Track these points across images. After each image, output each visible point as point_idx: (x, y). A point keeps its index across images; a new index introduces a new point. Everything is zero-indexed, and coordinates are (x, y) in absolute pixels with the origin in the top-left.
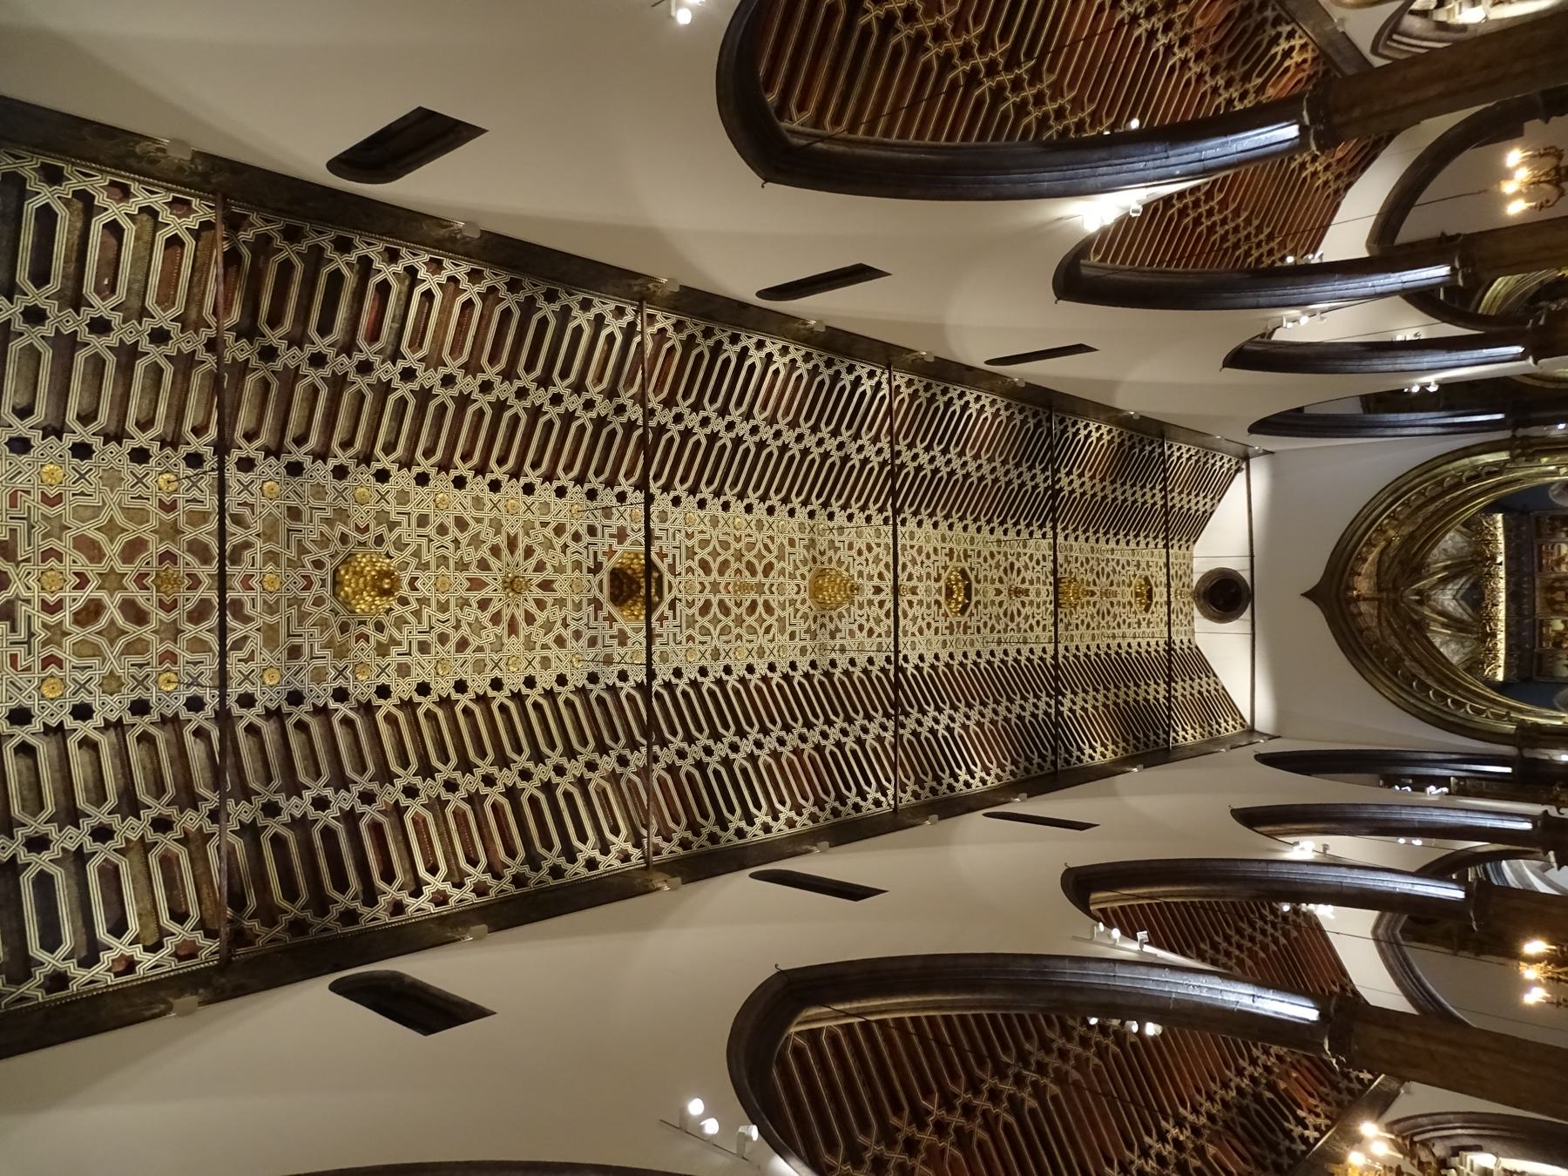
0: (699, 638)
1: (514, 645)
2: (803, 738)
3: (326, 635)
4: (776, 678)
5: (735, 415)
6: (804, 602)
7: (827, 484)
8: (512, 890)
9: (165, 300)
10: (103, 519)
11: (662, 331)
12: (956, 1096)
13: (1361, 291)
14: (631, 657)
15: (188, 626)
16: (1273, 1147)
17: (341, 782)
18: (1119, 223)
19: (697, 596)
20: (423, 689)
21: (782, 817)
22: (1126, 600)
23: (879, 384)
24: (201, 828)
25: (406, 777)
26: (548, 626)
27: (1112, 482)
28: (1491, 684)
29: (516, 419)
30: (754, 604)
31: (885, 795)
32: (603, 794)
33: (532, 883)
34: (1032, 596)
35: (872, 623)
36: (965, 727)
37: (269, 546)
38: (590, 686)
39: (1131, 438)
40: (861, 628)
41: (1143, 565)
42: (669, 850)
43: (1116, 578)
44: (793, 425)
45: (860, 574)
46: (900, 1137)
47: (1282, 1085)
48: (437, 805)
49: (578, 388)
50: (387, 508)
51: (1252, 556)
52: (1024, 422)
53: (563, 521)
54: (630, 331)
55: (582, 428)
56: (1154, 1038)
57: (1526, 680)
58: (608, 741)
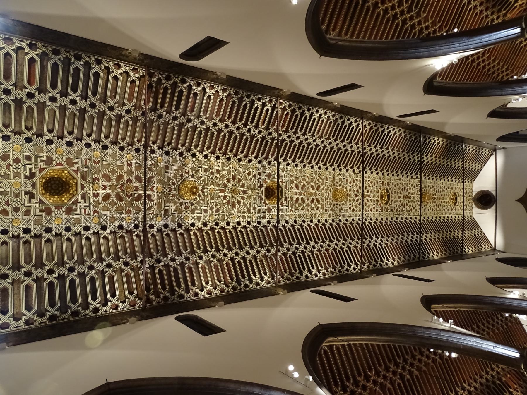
0: (294, 210)
1: (234, 211)
2: (329, 246)
3: (176, 206)
4: (320, 225)
5: (308, 135)
6: (330, 199)
7: (340, 159)
9: (130, 100)
10: (111, 168)
11: (284, 107)
12: (381, 372)
14: (272, 216)
15: (135, 202)
17: (180, 254)
18: (448, 66)
20: (205, 225)
22: (447, 201)
23: (358, 124)
24: (137, 266)
25: (199, 253)
27: (443, 159)
29: (236, 137)
30: (313, 200)
31: (357, 266)
32: (261, 261)
34: (412, 199)
35: (354, 207)
36: (386, 244)
37: (159, 178)
38: (258, 225)
39: (450, 143)
40: (350, 208)
41: (454, 188)
42: (283, 281)
43: (443, 193)
44: (328, 139)
45: (350, 190)
46: (360, 384)
47: (504, 379)
48: (209, 262)
49: (256, 127)
50: (195, 166)
51: (496, 186)
52: (410, 137)
54: (274, 108)
55: (257, 140)
56: (454, 358)
58: (264, 244)
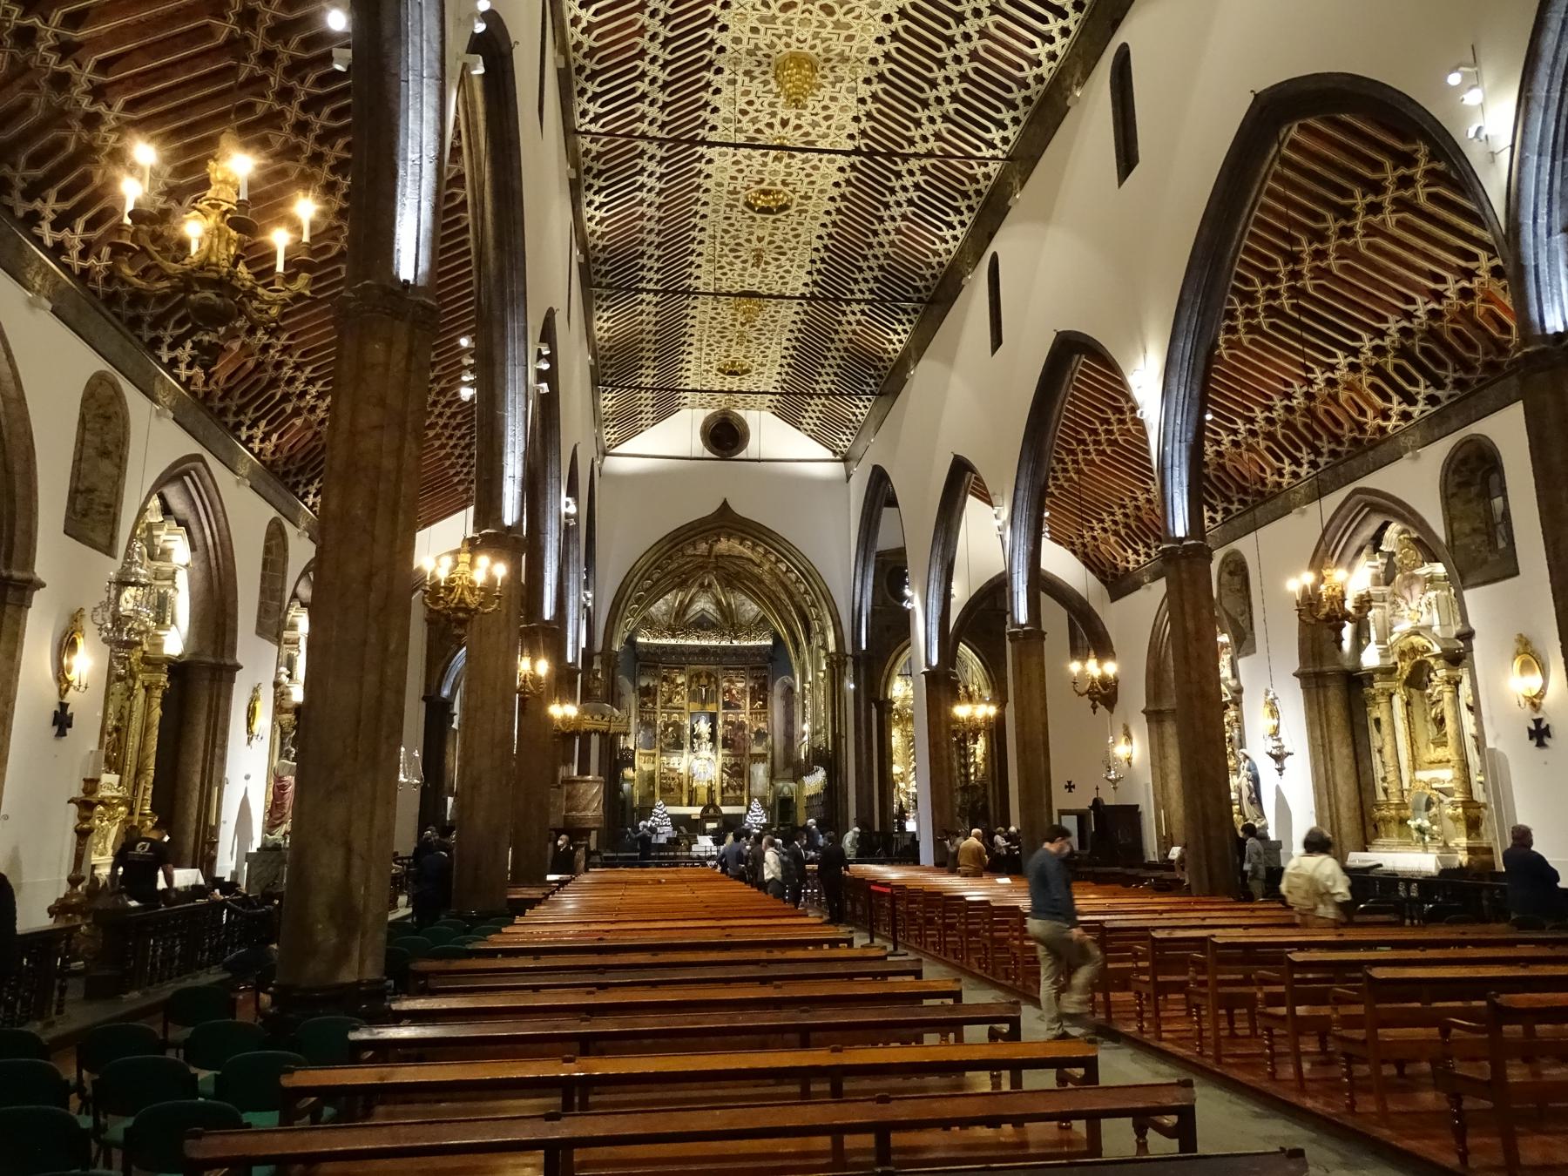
6: (788, 45)
13: (1015, 564)
16: (301, 471)
23: (994, 147)
27: (846, 349)
28: (634, 633)
31: (591, 122)
34: (751, 270)
35: (752, 114)
39: (885, 368)
40: (750, 103)
43: (753, 345)
45: (805, 107)
51: (759, 461)
52: (922, 277)
57: (637, 658)
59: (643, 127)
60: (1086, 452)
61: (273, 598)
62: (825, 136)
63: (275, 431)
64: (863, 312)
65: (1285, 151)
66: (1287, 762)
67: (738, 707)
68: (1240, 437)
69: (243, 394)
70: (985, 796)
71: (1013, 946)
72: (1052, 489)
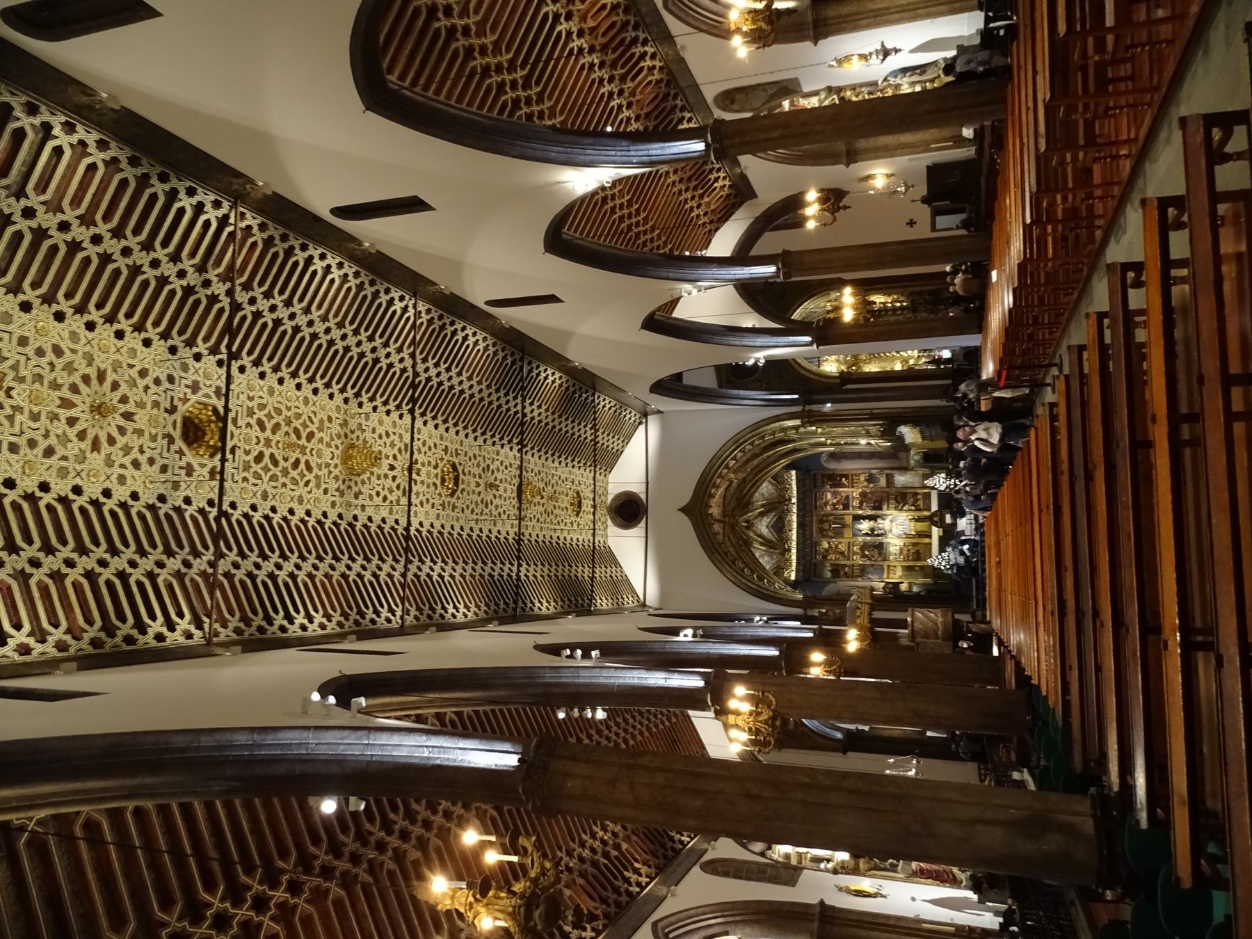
0: (252, 480)
1: (96, 460)
4: (311, 522)
5: (297, 307)
6: (336, 466)
7: (361, 379)
8: (90, 650)
11: (249, 227)
16: (663, 846)
19: (253, 446)
21: (316, 621)
23: (407, 306)
26: (127, 450)
27: (560, 416)
28: (787, 582)
30: (296, 464)
31: (394, 615)
32: (170, 587)
33: (107, 646)
36: (452, 576)
40: (378, 494)
43: (558, 489)
45: (380, 452)
46: (420, 817)
49: (175, 258)
52: (504, 358)
53: (147, 366)
55: (172, 293)
59: (397, 575)
60: (637, 224)
61: (764, 872)
62: (401, 436)
63: (632, 865)
64: (531, 404)
65: (407, 84)
66: (889, 46)
67: (847, 497)
68: (624, 103)
69: (605, 889)
70: (920, 293)
71: (1053, 267)
72: (667, 249)
